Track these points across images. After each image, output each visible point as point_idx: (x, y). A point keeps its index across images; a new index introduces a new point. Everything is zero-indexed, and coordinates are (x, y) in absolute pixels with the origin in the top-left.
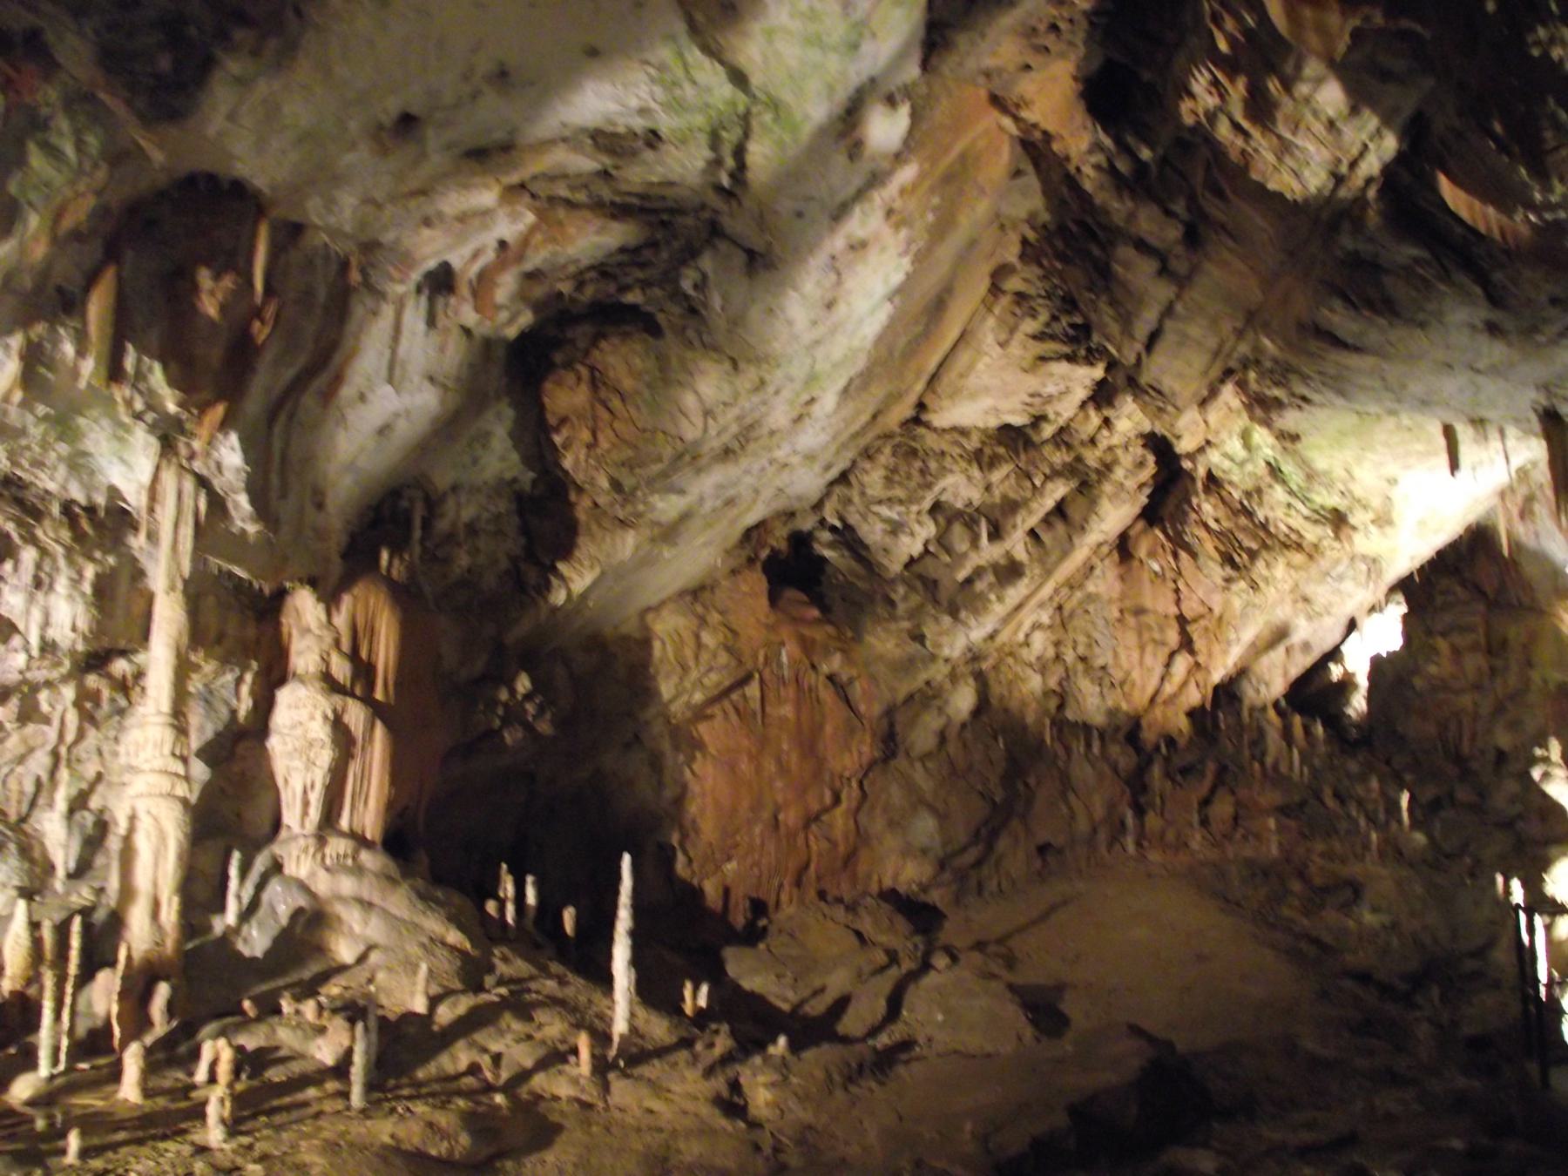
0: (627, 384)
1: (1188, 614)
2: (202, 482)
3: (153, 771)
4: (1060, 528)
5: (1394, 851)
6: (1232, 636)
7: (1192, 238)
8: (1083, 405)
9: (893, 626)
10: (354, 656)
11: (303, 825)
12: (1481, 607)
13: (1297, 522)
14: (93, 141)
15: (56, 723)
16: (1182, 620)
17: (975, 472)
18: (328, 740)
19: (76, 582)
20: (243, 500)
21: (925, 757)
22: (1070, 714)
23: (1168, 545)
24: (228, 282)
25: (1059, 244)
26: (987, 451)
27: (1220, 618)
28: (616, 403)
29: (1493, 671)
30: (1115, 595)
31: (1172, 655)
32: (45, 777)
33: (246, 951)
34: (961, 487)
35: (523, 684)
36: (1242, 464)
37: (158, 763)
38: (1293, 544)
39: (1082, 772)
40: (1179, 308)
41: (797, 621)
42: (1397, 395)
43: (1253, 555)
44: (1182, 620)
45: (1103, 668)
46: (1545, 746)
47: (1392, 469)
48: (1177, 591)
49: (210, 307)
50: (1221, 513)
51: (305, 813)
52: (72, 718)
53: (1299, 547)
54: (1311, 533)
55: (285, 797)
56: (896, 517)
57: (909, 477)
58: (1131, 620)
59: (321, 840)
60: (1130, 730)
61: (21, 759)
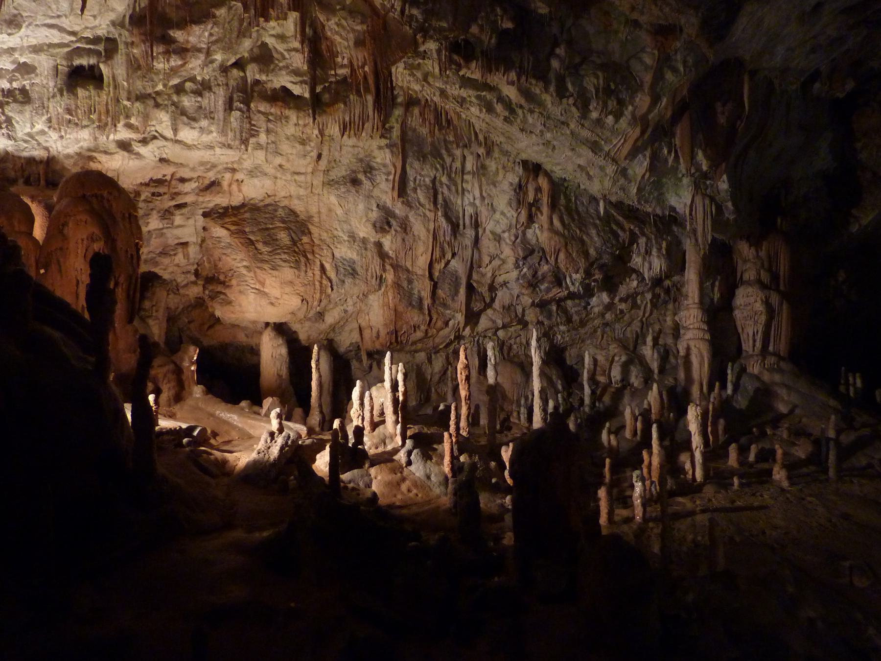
2: (712, 199)
10: (770, 270)
11: (754, 350)
14: (690, 61)
15: (642, 308)
18: (764, 311)
19: (659, 250)
32: (639, 331)
33: (738, 407)
37: (696, 325)
49: (722, 120)
51: (754, 346)
52: (649, 305)
55: (743, 337)
59: (764, 358)
61: (629, 325)
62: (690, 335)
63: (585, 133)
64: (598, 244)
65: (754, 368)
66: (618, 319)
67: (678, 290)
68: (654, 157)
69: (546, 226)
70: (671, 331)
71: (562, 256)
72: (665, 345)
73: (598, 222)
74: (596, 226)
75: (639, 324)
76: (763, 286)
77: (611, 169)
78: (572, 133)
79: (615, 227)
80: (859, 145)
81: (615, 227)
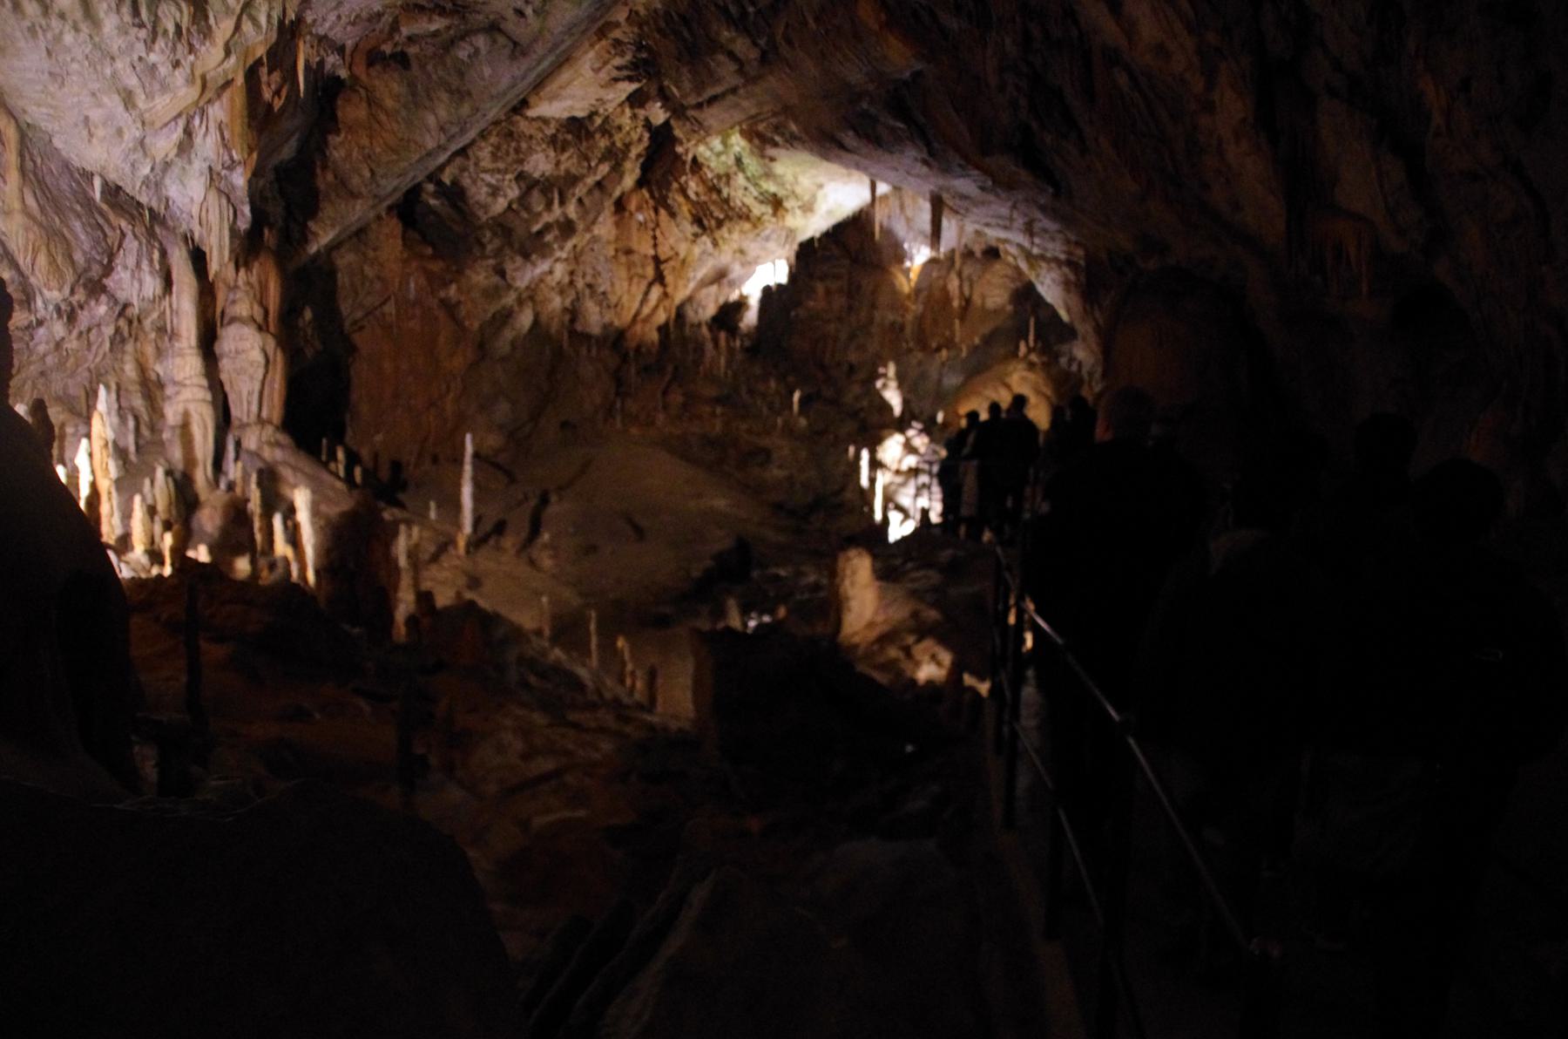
0: (389, 103)
1: (662, 257)
3: (193, 385)
4: (597, 194)
5: (789, 431)
6: (691, 275)
7: (764, 59)
8: (621, 105)
9: (485, 263)
10: (261, 304)
12: (847, 262)
13: (749, 201)
16: (657, 261)
17: (552, 154)
19: (151, 261)
20: (247, 210)
21: (503, 359)
22: (579, 328)
23: (651, 202)
24: (276, 76)
25: (662, 24)
26: (560, 136)
27: (684, 261)
28: (383, 117)
29: (850, 308)
30: (612, 238)
31: (650, 285)
34: (541, 164)
35: (308, 314)
36: (719, 155)
38: (745, 216)
39: (587, 371)
40: (741, 91)
41: (422, 257)
42: (858, 167)
43: (720, 224)
44: (657, 261)
45: (604, 293)
46: (885, 366)
47: (821, 179)
48: (655, 238)
50: (701, 189)
52: (107, 345)
53: (748, 218)
54: (757, 209)
55: (232, 398)
56: (493, 182)
57: (508, 154)
58: (623, 259)
60: (616, 339)
62: (187, 394)
63: (132, 82)
64: (86, 247)
65: (251, 441)
66: (61, 365)
67: (139, 321)
68: (188, 132)
69: (17, 205)
70: (137, 387)
71: (42, 259)
72: (132, 409)
73: (78, 208)
74: (79, 216)
75: (86, 374)
76: (260, 328)
77: (133, 132)
78: (114, 74)
79: (101, 221)
80: (334, 140)
81: (101, 221)
